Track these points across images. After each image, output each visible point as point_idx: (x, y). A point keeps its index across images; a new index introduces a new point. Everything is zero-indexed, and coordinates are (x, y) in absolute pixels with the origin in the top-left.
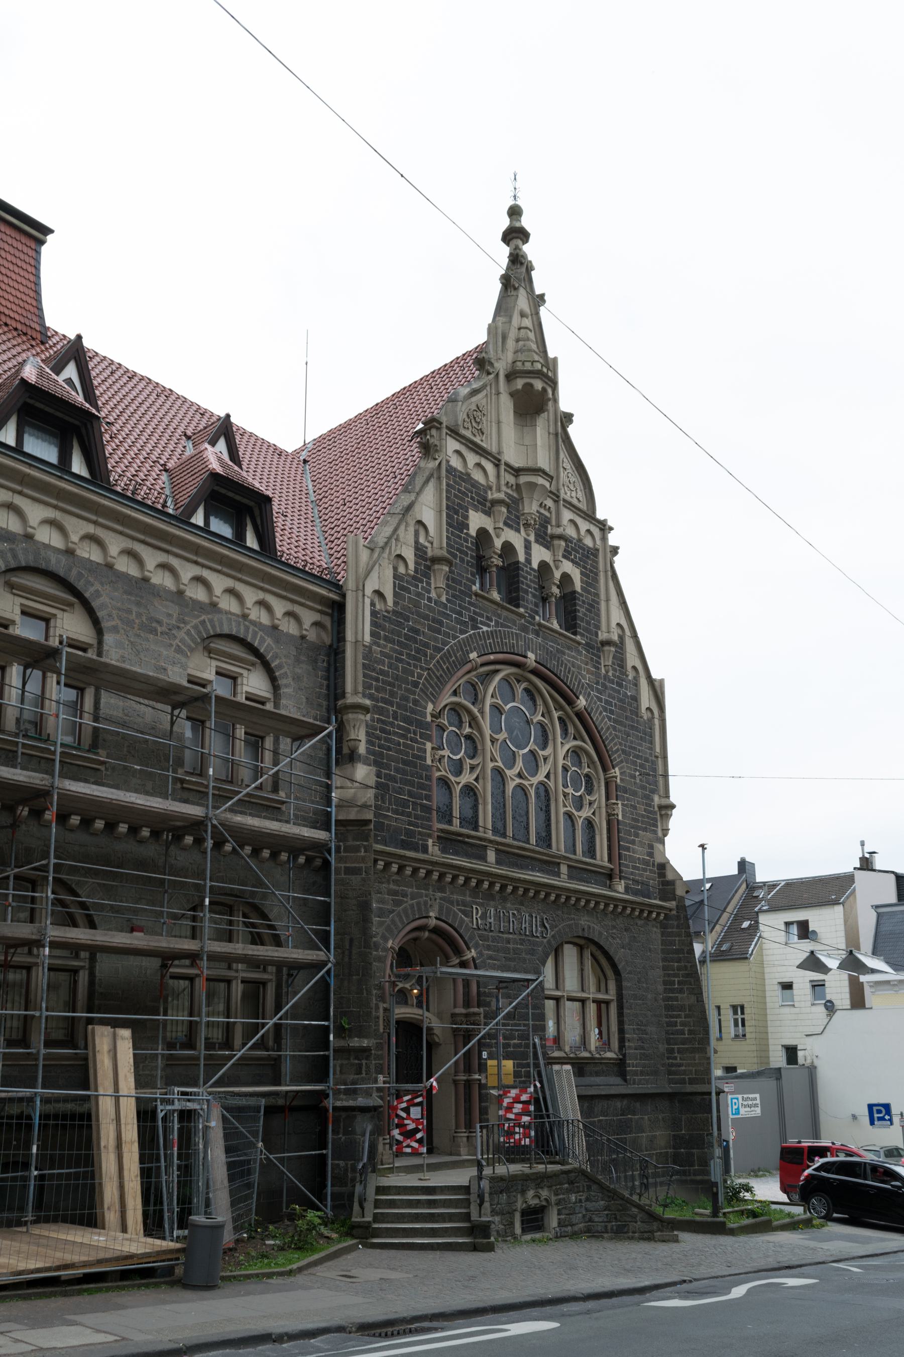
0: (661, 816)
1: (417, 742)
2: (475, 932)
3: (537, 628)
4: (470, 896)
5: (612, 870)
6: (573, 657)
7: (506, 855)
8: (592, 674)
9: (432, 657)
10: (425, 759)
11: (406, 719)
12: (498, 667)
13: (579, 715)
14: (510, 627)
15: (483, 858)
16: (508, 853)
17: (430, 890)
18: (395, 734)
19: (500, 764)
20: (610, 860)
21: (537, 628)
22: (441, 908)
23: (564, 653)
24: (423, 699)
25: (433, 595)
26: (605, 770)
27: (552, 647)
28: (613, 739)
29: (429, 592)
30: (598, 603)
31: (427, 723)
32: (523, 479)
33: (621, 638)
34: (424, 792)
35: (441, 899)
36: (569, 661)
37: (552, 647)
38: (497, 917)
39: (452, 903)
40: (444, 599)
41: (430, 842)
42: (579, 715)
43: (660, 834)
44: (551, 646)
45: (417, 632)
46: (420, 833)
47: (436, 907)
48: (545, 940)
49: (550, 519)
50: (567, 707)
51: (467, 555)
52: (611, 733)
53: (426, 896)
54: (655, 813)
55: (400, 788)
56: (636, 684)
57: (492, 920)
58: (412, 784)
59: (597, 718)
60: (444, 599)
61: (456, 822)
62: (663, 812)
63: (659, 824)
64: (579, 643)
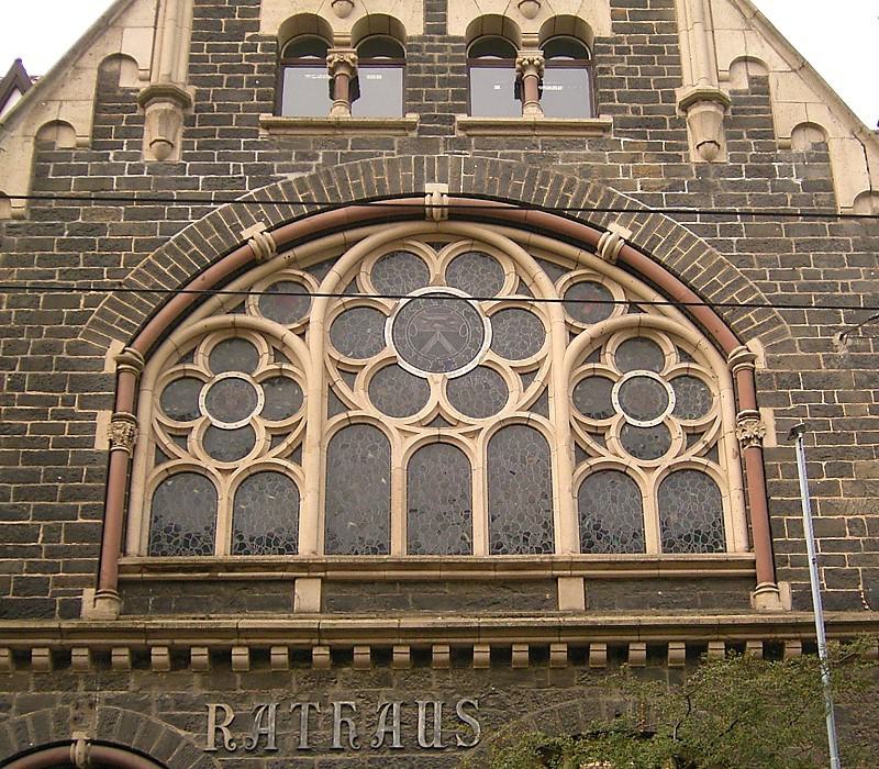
1: (73, 416)
2: (216, 761)
3: (459, 134)
4: (203, 686)
5: (753, 564)
6: (587, 157)
7: (342, 587)
8: (657, 173)
11: (38, 384)
12: (351, 234)
14: (372, 155)
15: (286, 605)
16: (372, 582)
17: (82, 686)
19: (370, 410)
20: (750, 547)
21: (459, 134)
22: (107, 721)
23: (552, 159)
24: (96, 337)
25: (148, 156)
27: (512, 156)
28: (741, 281)
29: (137, 156)
31: (108, 376)
33: (761, 87)
34: (81, 504)
35: (108, 701)
36: (569, 169)
37: (512, 156)
38: (281, 723)
39: (144, 706)
40: (176, 157)
41: (89, 594)
42: (622, 263)
44: (503, 156)
45: (100, 229)
46: (58, 582)
47: (94, 720)
48: (466, 755)
50: (586, 256)
51: (250, 69)
52: (731, 273)
53: (66, 701)
55: (15, 507)
56: (821, 155)
57: (271, 728)
58: (49, 494)
59: (676, 254)
60: (176, 157)
61: (222, 548)
64: (605, 128)
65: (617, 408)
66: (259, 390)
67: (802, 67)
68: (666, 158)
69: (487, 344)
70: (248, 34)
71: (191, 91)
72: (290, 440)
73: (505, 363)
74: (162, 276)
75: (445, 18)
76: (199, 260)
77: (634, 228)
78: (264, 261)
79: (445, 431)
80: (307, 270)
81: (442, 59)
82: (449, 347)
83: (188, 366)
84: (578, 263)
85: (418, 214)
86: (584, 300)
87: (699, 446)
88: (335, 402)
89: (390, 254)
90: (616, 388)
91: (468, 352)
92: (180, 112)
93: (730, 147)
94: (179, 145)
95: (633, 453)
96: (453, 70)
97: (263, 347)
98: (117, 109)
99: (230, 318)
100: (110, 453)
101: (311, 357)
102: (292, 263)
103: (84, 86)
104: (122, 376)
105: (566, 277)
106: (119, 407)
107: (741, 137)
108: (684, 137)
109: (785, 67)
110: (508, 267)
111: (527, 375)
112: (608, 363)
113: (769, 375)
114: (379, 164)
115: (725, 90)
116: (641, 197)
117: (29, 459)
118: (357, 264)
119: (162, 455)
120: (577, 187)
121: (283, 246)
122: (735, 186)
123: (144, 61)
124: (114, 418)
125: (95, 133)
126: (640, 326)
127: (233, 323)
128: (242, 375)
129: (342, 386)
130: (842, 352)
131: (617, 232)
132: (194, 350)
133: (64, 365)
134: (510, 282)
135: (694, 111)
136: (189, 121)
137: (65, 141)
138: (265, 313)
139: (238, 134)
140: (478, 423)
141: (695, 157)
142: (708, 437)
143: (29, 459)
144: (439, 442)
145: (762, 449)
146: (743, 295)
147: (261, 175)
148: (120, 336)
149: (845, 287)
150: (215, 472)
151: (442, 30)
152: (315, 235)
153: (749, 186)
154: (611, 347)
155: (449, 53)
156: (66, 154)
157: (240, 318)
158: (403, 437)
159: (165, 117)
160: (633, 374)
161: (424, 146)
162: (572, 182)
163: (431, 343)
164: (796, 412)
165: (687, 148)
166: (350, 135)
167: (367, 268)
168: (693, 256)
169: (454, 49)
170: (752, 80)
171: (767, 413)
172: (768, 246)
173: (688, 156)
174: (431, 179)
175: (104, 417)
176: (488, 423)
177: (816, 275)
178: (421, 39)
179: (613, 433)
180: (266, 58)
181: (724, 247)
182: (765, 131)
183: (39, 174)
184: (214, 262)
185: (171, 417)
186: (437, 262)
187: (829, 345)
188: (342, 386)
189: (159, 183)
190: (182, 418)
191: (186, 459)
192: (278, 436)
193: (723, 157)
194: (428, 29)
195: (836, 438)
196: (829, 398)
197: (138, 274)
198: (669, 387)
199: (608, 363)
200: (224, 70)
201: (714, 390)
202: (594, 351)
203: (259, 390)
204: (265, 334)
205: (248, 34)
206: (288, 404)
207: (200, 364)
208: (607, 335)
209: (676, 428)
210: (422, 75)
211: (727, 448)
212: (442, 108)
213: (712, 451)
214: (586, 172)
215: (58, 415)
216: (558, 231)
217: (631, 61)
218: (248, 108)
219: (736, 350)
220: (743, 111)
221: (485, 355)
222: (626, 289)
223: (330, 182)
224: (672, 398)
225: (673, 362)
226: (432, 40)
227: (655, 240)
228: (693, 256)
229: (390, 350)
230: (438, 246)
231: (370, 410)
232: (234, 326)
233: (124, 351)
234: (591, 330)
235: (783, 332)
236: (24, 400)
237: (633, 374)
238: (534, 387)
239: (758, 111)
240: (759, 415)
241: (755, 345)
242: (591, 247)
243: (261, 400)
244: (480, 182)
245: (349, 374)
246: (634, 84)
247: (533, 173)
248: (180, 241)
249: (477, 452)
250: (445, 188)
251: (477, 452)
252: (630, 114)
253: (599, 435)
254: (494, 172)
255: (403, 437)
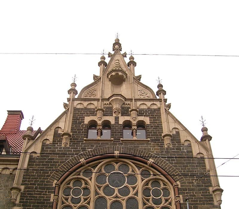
0: (215, 195)
6: (145, 146)
8: (159, 149)
9: (59, 165)
10: (50, 200)
12: (100, 161)
13: (152, 166)
14: (105, 146)
18: (35, 194)
19: (103, 195)
25: (63, 146)
26: (172, 184)
27: (131, 146)
29: (61, 146)
30: (162, 125)
32: (110, 100)
33: (178, 133)
36: (142, 149)
37: (131, 146)
40: (68, 146)
42: (152, 166)
43: (216, 203)
44: (129, 146)
45: (53, 159)
49: (130, 107)
50: (145, 165)
52: (173, 169)
54: (211, 195)
56: (190, 146)
60: (68, 146)
62: (215, 193)
63: (214, 199)
64: (149, 141)
65: (152, 195)
66: (82, 190)
67: (186, 129)
68: (160, 147)
69: (126, 182)
70: (82, 123)
71: (71, 134)
72: (88, 200)
73: (130, 186)
74: (64, 168)
75: (118, 121)
76: (72, 165)
77: (154, 160)
78: (84, 166)
79: (118, 199)
80: (92, 167)
81: (118, 128)
82: (119, 183)
83: (69, 186)
84: (144, 167)
85: (113, 157)
86: (145, 174)
87: (168, 203)
88: (97, 193)
89: (108, 165)
90: (151, 191)
91: (122, 184)
92: (69, 137)
93: (172, 145)
94: (69, 144)
95: (154, 204)
96: (120, 130)
97: (83, 182)
98: (57, 137)
99: (77, 176)
100: (53, 202)
101: (92, 184)
102: (89, 166)
103: (52, 132)
104: (56, 187)
105: (142, 169)
106: (55, 193)
107: (174, 143)
108: (164, 143)
109: (182, 129)
110: (130, 167)
111: (134, 188)
112: (150, 186)
113: (181, 188)
114: (106, 148)
115: (171, 134)
116: (156, 154)
117: (38, 203)
118: (101, 166)
119: (63, 203)
120: (143, 152)
121: (87, 163)
122: (174, 152)
123: (63, 128)
124: (54, 195)
125: (53, 141)
126: (156, 179)
127: (78, 177)
128: (79, 188)
129: (98, 190)
130: (195, 184)
131: (151, 161)
132: (70, 182)
133: (45, 185)
134: (131, 170)
135: (165, 138)
136: (71, 139)
137: (48, 143)
138: (84, 176)
139: (80, 142)
140: (124, 197)
141: (166, 146)
142: (169, 201)
143: (38, 203)
144: (117, 201)
145: (180, 203)
146: (176, 173)
147: (84, 149)
148: (56, 179)
149: (195, 171)
150: (73, 206)
151: (118, 123)
152: (93, 161)
153: (177, 152)
154: (150, 183)
155: (119, 127)
156: (48, 145)
157: (79, 176)
158: (109, 200)
159: (66, 138)
160: (154, 188)
161: (114, 144)
162: (142, 151)
163: (115, 182)
164: (186, 196)
165: (164, 145)
166: (101, 142)
167: (103, 167)
168: (166, 165)
169: (120, 126)
170: (176, 132)
171: (181, 196)
172: (180, 163)
173: (164, 146)
174: (116, 150)
175: (52, 195)
176: (126, 198)
177: (190, 169)
178: (114, 124)
179: (151, 200)
180: (85, 128)
181: (172, 163)
182: (179, 141)
183: (42, 149)
184: (74, 166)
185: (65, 195)
186: (116, 166)
187: (193, 183)
188: (98, 190)
189: (65, 151)
190: (67, 196)
191: (67, 204)
192: (85, 199)
193: (171, 146)
194: (115, 123)
195: (194, 201)
196: (193, 193)
197: (60, 168)
198: (161, 191)
199: (150, 186)
200: (77, 130)
201: (170, 191)
202: (147, 184)
203: (82, 190)
204: (84, 180)
205: (82, 123)
206: (87, 193)
207: (71, 185)
208: (149, 180)
209: (163, 198)
210: (114, 131)
211: (173, 203)
212: (118, 137)
213: (170, 204)
214: (145, 149)
215: (43, 194)
216: (139, 160)
217: (153, 128)
218: (82, 137)
219: (175, 184)
220: (175, 138)
221: (126, 184)
222: (153, 172)
223: (96, 151)
224: (162, 193)
225: (162, 186)
226: (116, 125)
227: (158, 162)
228: (166, 165)
229: (107, 183)
230: (117, 163)
231: (103, 195)
232: (78, 178)
233: (57, 182)
234: (146, 180)
235: (184, 180)
236: (37, 191)
237: (154, 188)
238: (135, 190)
239: (178, 138)
240: (179, 197)
241: (178, 183)
242: (146, 163)
243: (82, 192)
244: (125, 151)
245: (99, 188)
246: (154, 133)
247: (135, 149)
248: (68, 161)
249: (124, 203)
250: (118, 152)
251: (124, 203)
252: (153, 138)
253: (148, 200)
254: (128, 149)
255: (109, 200)
